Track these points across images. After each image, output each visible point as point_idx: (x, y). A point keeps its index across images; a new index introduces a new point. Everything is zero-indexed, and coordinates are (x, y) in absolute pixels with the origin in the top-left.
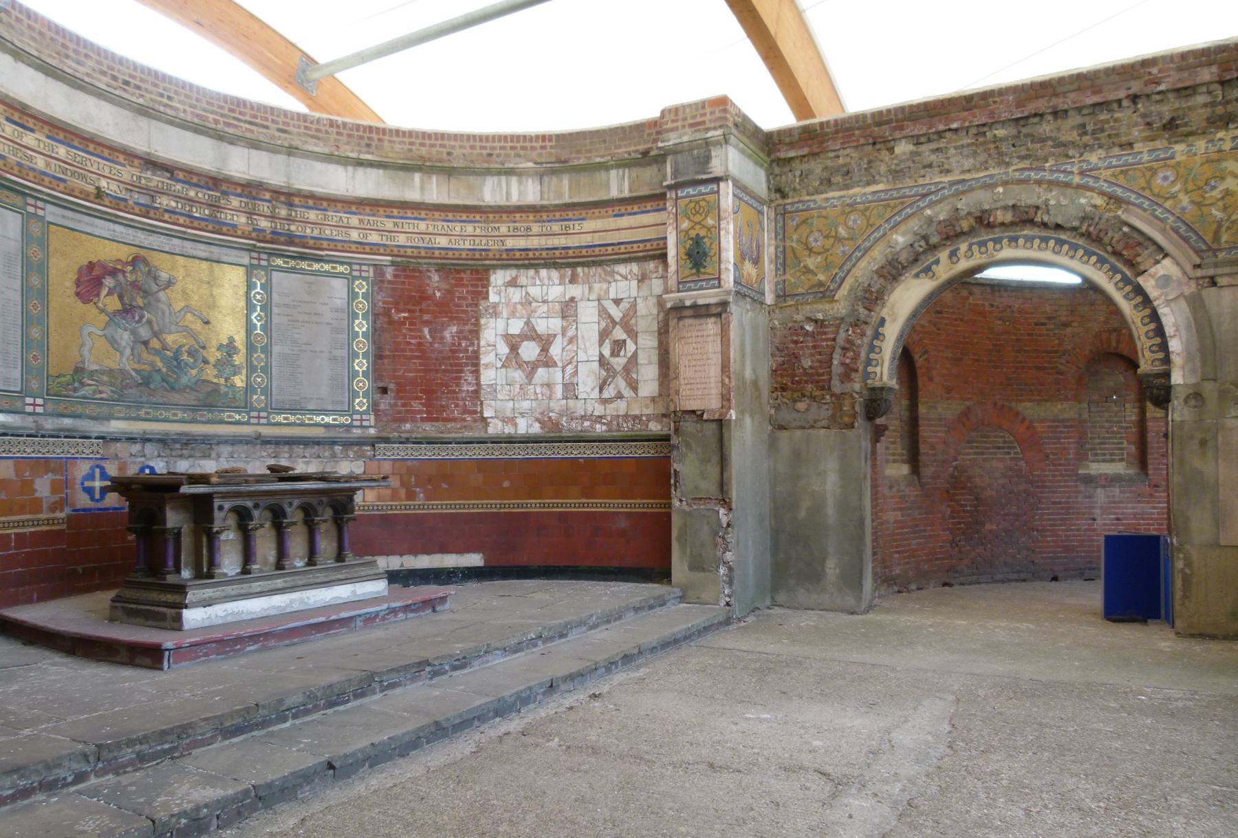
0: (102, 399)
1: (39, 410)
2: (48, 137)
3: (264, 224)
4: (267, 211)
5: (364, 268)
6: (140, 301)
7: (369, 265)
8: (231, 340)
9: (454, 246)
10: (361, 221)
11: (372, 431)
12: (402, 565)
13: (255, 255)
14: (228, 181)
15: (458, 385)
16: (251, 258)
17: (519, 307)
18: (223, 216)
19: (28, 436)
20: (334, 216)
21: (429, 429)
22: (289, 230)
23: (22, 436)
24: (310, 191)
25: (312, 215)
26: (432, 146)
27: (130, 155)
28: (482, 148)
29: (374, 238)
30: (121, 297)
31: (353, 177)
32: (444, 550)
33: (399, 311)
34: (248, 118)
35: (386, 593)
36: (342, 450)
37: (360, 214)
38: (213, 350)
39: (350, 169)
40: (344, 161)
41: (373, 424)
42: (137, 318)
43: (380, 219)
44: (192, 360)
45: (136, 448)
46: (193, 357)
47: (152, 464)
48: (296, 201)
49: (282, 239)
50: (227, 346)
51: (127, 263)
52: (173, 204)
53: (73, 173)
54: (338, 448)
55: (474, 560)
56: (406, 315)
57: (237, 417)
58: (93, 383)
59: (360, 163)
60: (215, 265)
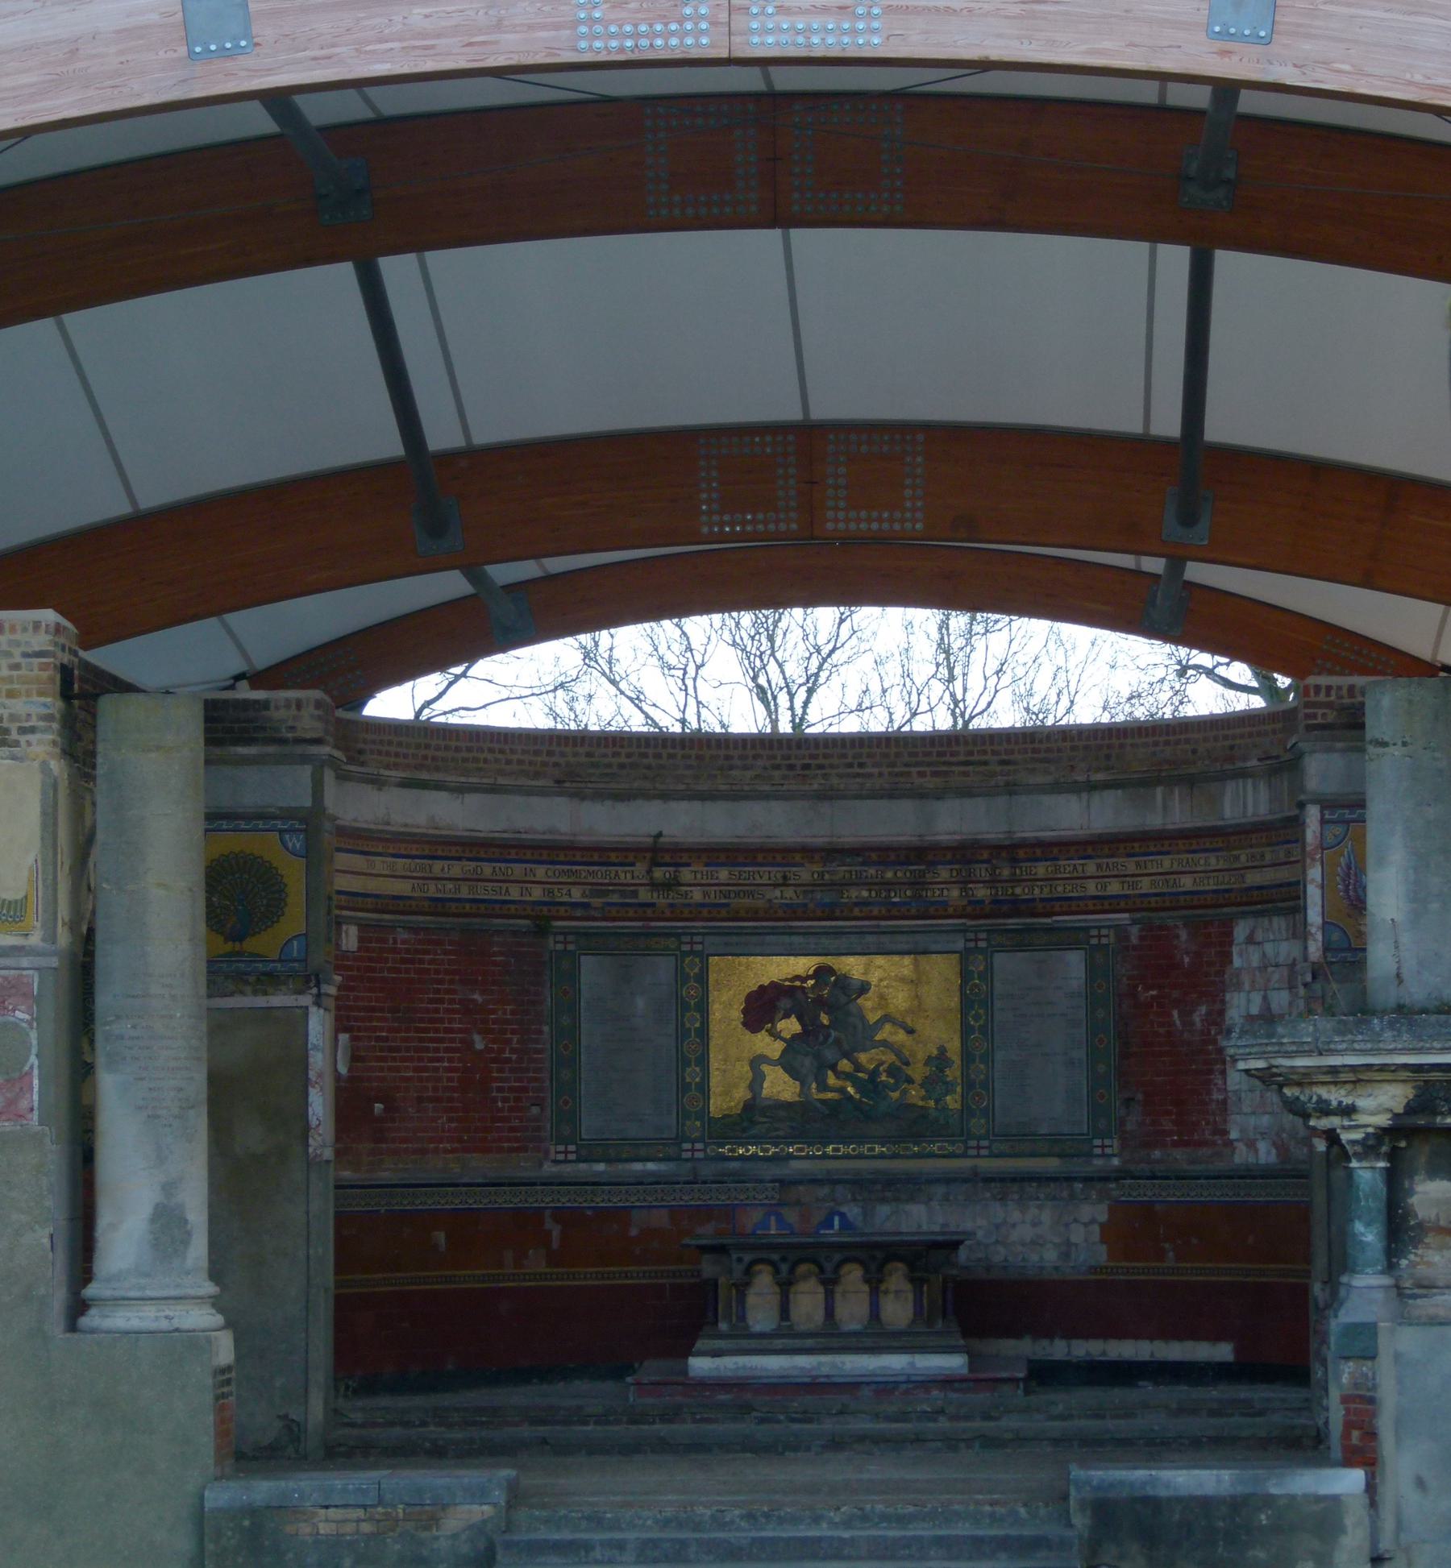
0: (778, 1137)
1: (700, 1155)
2: (707, 865)
3: (981, 892)
4: (985, 875)
5: (1104, 932)
6: (825, 1019)
7: (1109, 927)
8: (942, 1050)
9: (1201, 888)
10: (1099, 866)
11: (1116, 1162)
12: (1152, 1355)
13: (971, 936)
14: (936, 848)
15: (1209, 1093)
16: (966, 940)
17: (1257, 973)
18: (934, 894)
19: (684, 1183)
20: (1067, 866)
21: (1180, 1157)
22: (1013, 894)
23: (678, 1183)
24: (1036, 838)
25: (1041, 869)
26: (1178, 742)
27: (808, 852)
28: (1226, 737)
29: (1114, 888)
30: (800, 1019)
31: (1088, 806)
32: (1194, 1335)
33: (1147, 988)
34: (962, 758)
35: (965, 1371)
36: (1082, 1190)
37: (1099, 857)
38: (920, 1065)
39: (1084, 795)
40: (1076, 788)
41: (1116, 1151)
42: (821, 1038)
43: (1121, 860)
44: (892, 1081)
45: (824, 1191)
46: (893, 1077)
47: (844, 1209)
48: (1021, 854)
49: (1005, 908)
50: (937, 1058)
51: (809, 977)
52: (865, 894)
53: (737, 894)
54: (1079, 1186)
55: (1223, 1352)
56: (1154, 993)
57: (951, 1149)
58: (764, 1120)
59: (1092, 787)
60: (921, 958)
